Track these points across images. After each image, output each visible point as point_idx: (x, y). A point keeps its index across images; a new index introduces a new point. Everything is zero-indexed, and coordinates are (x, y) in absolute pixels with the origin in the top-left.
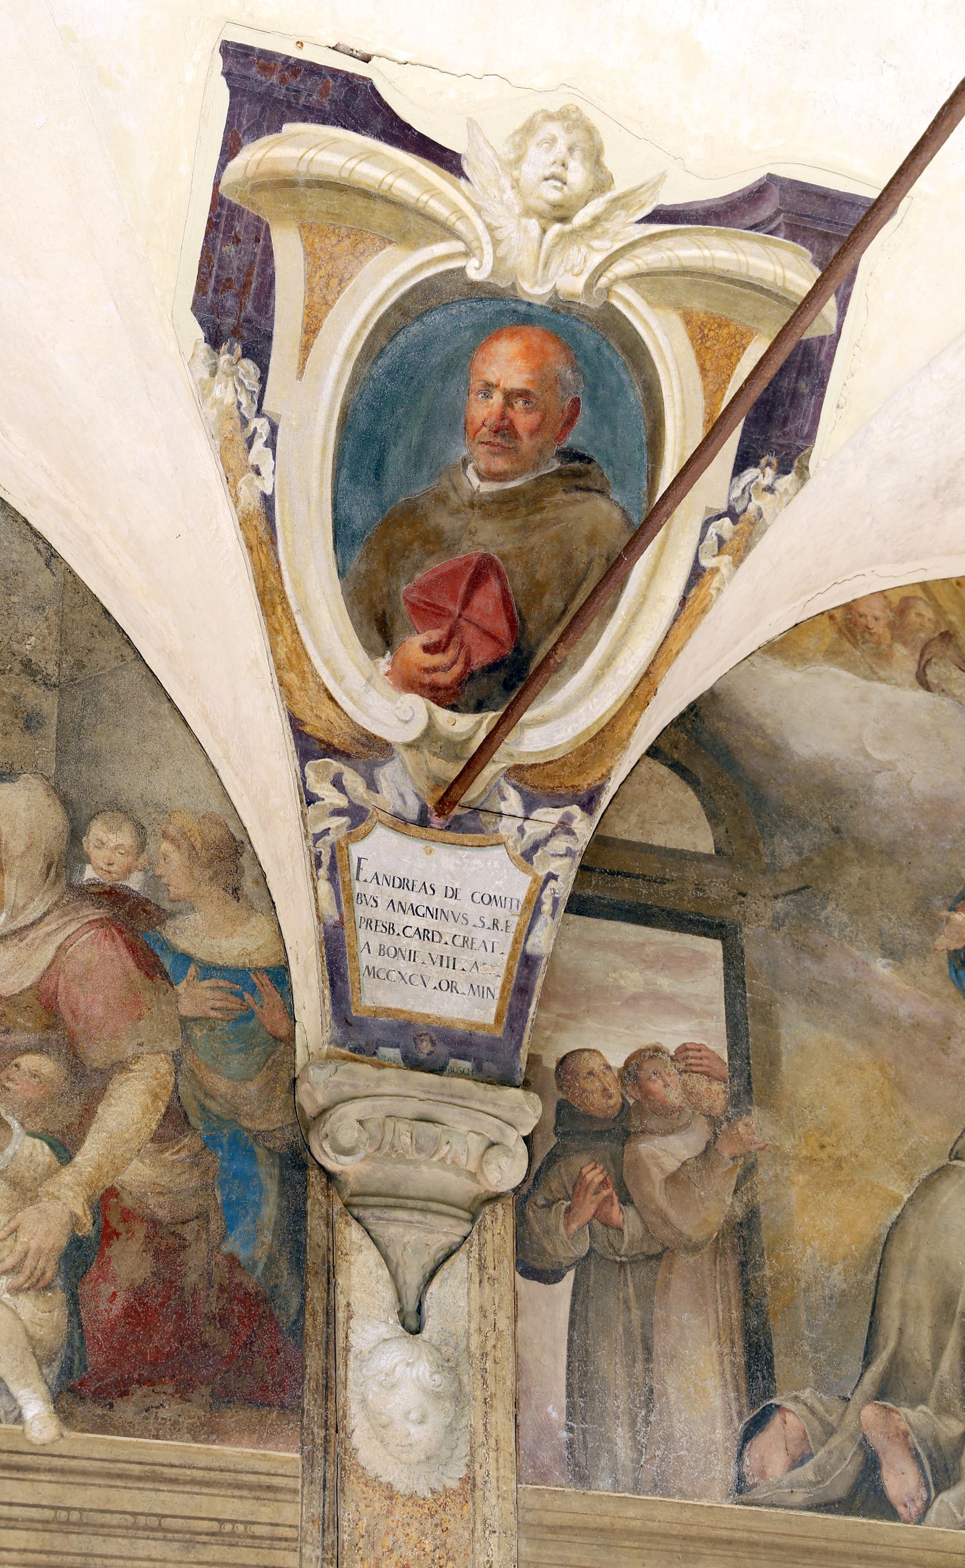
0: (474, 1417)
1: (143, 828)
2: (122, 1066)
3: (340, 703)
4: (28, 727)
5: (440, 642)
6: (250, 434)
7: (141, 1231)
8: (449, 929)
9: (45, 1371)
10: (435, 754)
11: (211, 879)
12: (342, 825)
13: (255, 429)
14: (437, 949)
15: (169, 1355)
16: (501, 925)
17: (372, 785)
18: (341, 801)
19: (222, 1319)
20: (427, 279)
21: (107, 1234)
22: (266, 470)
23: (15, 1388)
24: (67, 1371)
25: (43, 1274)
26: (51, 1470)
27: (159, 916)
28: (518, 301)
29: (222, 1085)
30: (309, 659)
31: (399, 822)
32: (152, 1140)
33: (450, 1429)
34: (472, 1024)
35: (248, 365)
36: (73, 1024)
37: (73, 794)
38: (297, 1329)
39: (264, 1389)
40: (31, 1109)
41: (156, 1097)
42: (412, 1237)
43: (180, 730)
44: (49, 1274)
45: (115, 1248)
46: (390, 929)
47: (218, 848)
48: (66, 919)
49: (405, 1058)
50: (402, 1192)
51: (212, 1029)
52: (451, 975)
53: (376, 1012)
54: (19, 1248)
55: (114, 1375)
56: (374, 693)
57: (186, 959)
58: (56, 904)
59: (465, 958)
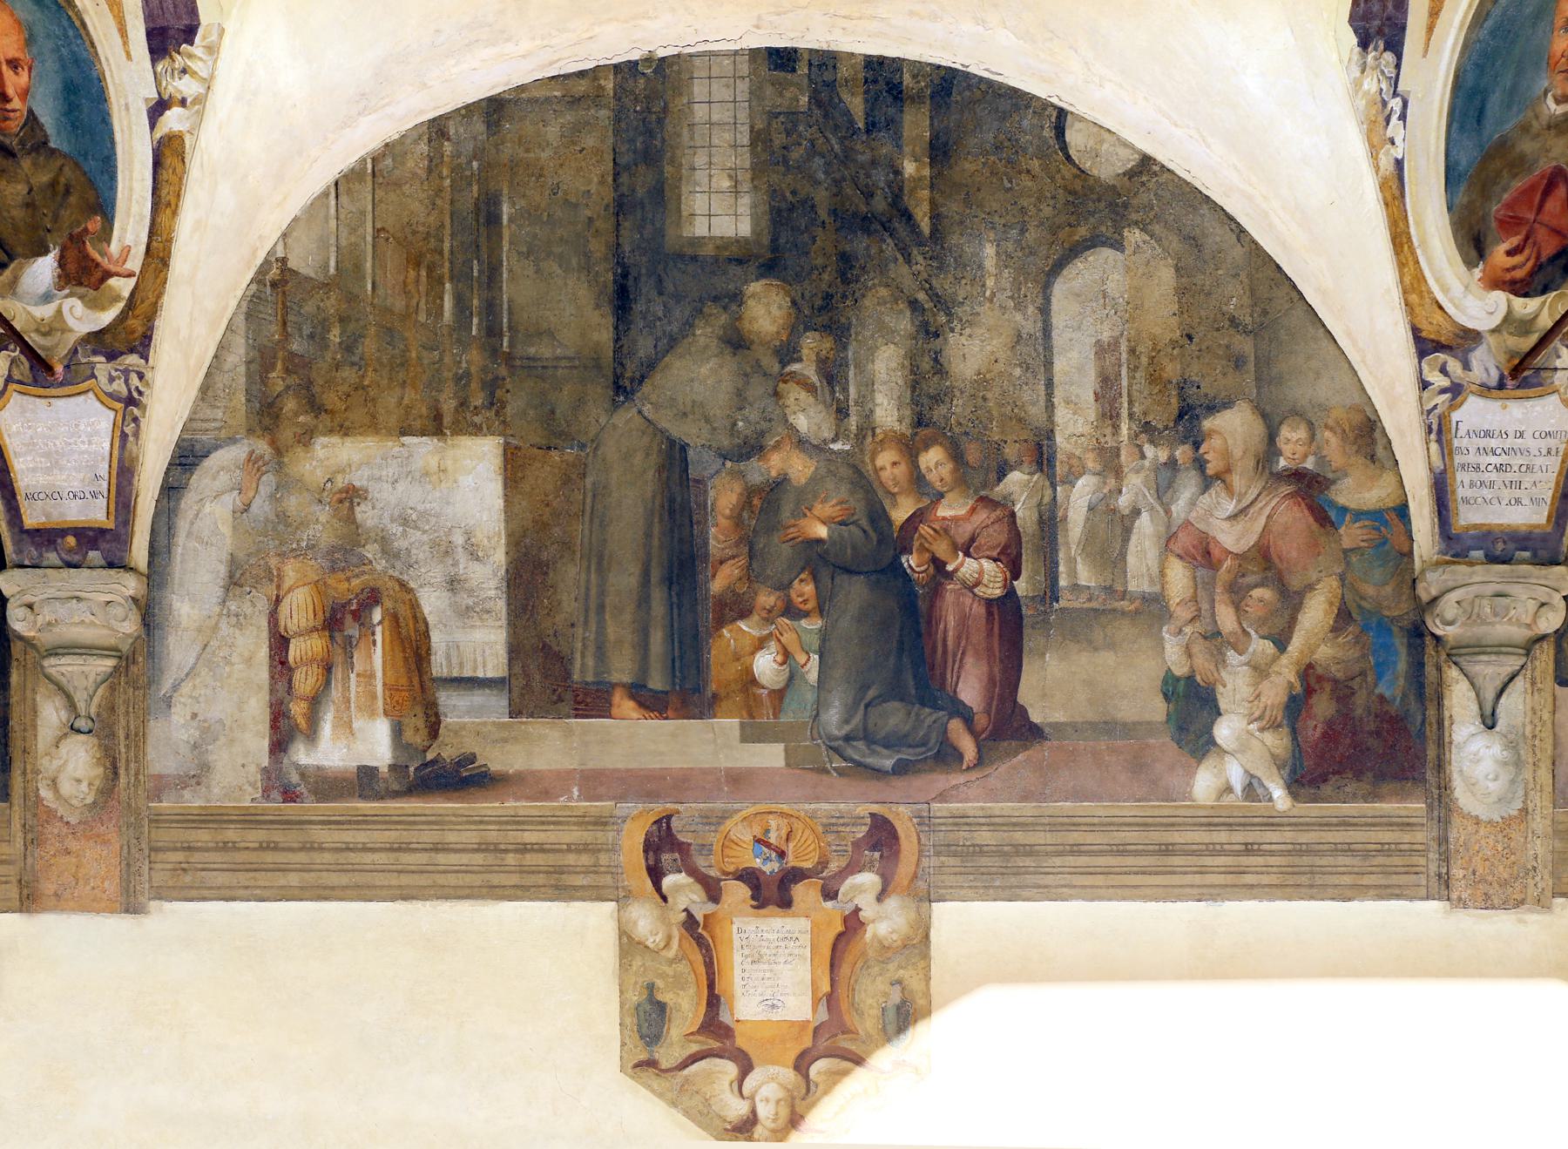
0: (1527, 774)
2: (1310, 587)
4: (1237, 367)
7: (1328, 687)
8: (1516, 461)
14: (1509, 476)
15: (1348, 757)
16: (1553, 452)
19: (1378, 733)
21: (1309, 691)
23: (1266, 783)
24: (1293, 771)
26: (1290, 825)
29: (1370, 590)
33: (1513, 782)
34: (1531, 526)
36: (1280, 566)
37: (1268, 408)
38: (1422, 734)
39: (1403, 770)
40: (1261, 622)
41: (1331, 604)
42: (1490, 670)
43: (1331, 347)
45: (1314, 700)
46: (1477, 468)
47: (1360, 429)
49: (1486, 556)
50: (1484, 643)
51: (1362, 555)
52: (1518, 493)
53: (1467, 528)
54: (1262, 705)
55: (1320, 770)
56: (1470, 297)
57: (1344, 510)
59: (1528, 480)
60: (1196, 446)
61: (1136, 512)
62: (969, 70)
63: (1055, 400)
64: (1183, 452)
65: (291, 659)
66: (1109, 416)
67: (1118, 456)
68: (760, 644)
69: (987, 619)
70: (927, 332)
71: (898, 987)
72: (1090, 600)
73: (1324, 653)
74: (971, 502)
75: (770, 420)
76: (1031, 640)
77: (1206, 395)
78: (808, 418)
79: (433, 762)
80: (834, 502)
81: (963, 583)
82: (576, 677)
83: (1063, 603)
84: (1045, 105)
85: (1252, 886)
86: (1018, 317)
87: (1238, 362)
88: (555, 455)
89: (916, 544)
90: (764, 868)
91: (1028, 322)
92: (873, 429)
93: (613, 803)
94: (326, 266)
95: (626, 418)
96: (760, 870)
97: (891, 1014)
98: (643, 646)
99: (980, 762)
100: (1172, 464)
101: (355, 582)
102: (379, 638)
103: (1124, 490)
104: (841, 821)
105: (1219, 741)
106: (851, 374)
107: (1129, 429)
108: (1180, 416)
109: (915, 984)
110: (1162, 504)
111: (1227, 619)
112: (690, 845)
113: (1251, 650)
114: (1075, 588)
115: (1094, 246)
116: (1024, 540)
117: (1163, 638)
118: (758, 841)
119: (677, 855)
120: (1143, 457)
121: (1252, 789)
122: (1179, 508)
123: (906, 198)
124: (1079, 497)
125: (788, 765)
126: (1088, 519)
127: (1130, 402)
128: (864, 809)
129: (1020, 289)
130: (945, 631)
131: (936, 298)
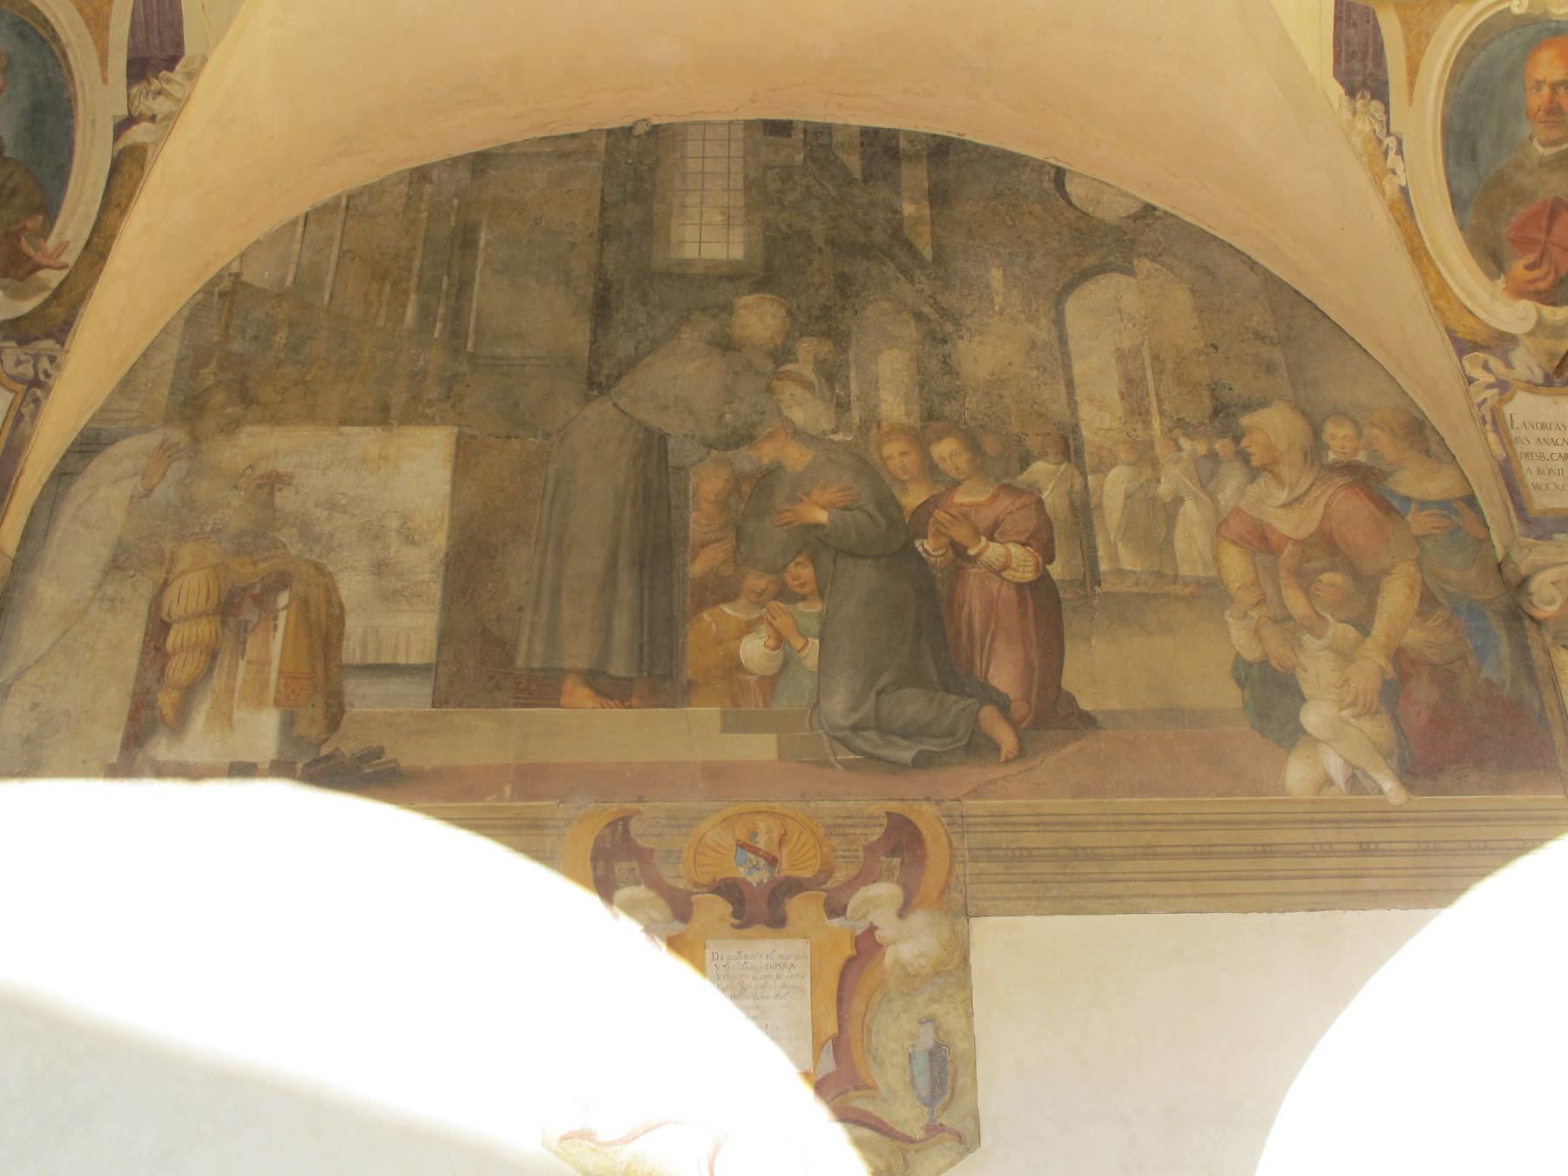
1: (1357, 422)
2: (1386, 572)
3: (1477, 314)
5: (1536, 261)
6: (1384, 149)
9: (1389, 762)
10: (1546, 337)
11: (1409, 447)
12: (1494, 395)
13: (1388, 145)
17: (1509, 365)
18: (1491, 379)
20: (1485, 21)
21: (1404, 677)
22: (1399, 170)
23: (1372, 774)
25: (1371, 705)
26: (1409, 820)
27: (1383, 476)
28: (1550, 21)
30: (1450, 289)
31: (1531, 386)
32: (1417, 615)
35: (1376, 105)
41: (1412, 588)
44: (1375, 706)
46: (1542, 456)
48: (1325, 487)
53: (1546, 512)
57: (1408, 500)
58: (1316, 478)
60: (1237, 440)
61: (1178, 501)
62: (963, 138)
63: (1078, 399)
64: (1222, 446)
65: (169, 645)
66: (1137, 410)
67: (1152, 447)
68: (749, 628)
69: (1019, 604)
70: (934, 339)
71: (929, 1027)
72: (1137, 584)
73: (1414, 637)
74: (991, 490)
75: (762, 413)
76: (1072, 624)
77: (1240, 396)
78: (805, 410)
79: (328, 757)
80: (836, 488)
81: (989, 568)
82: (520, 662)
83: (1105, 587)
84: (1042, 166)
85: (1376, 893)
86: (1031, 328)
87: (1270, 368)
88: (515, 444)
89: (931, 529)
90: (749, 879)
91: (1043, 332)
92: (879, 423)
93: (554, 803)
94: (283, 279)
95: (600, 409)
96: (744, 881)
97: (922, 1062)
98: (606, 630)
99: (1021, 753)
100: (1212, 456)
101: (263, 567)
102: (281, 623)
103: (1163, 480)
104: (850, 822)
105: (1309, 729)
106: (852, 374)
107: (1162, 424)
108: (1215, 413)
109: (952, 1021)
110: (1207, 493)
111: (1297, 603)
112: (652, 851)
113: (1330, 634)
114: (1119, 572)
115: (1105, 272)
116: (1055, 526)
117: (1226, 623)
118: (742, 846)
119: (635, 864)
120: (1180, 449)
121: (1355, 780)
122: (1227, 495)
123: (906, 232)
124: (1114, 487)
125: (781, 757)
126: (1125, 507)
127: (1159, 401)
128: (877, 808)
129: (1030, 305)
130: (970, 614)
131: (944, 313)
